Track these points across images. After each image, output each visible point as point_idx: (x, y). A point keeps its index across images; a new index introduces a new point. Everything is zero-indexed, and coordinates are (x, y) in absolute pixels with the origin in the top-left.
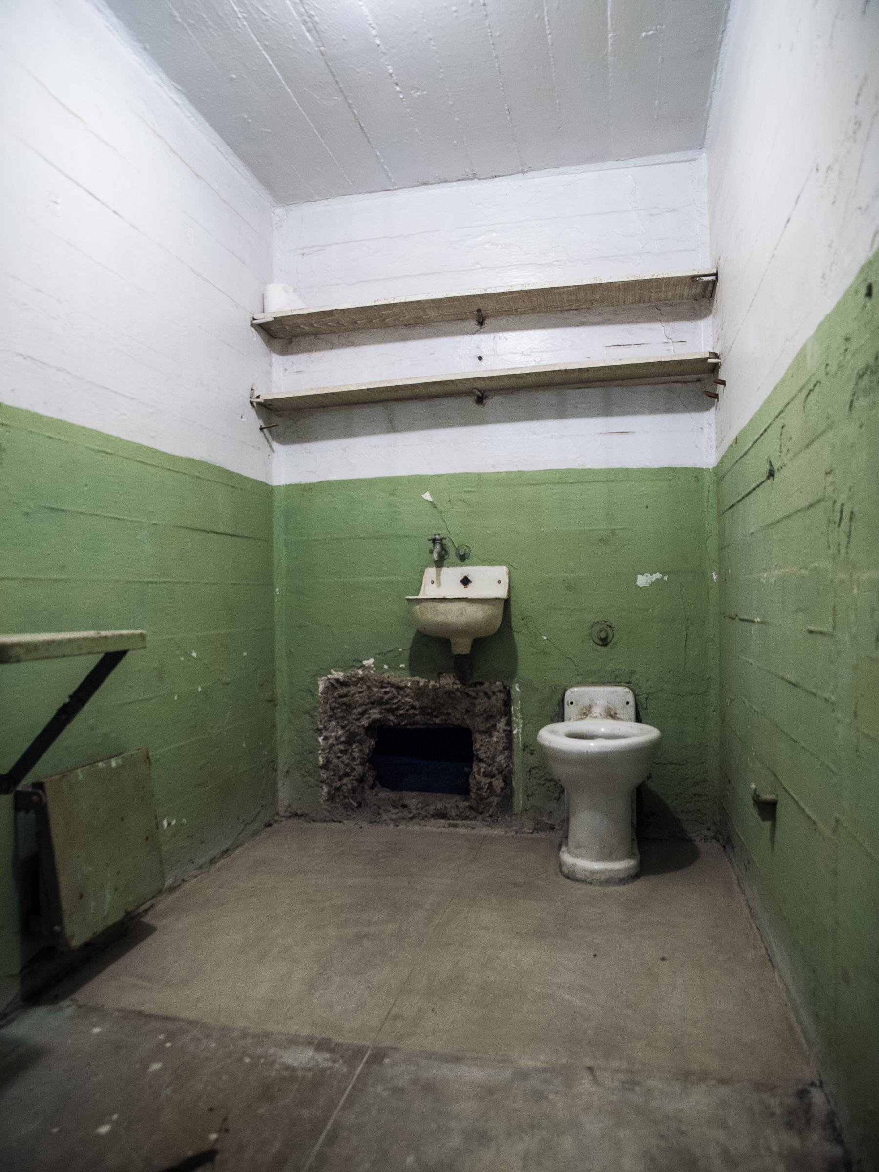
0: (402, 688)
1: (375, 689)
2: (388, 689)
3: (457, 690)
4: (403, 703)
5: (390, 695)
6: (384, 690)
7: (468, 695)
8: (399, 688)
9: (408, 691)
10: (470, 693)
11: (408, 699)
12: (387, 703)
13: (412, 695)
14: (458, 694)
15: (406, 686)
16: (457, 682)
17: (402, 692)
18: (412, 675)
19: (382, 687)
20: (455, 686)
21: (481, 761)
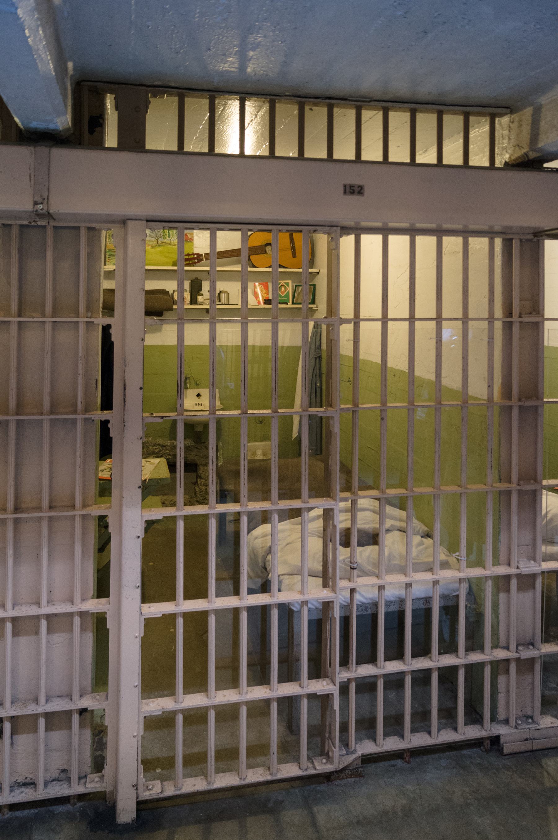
0: (165, 446)
1: (151, 447)
2: (157, 447)
3: (192, 446)
4: (165, 453)
5: (158, 450)
6: (155, 447)
7: (197, 448)
8: (163, 446)
9: (167, 447)
10: (198, 447)
11: (167, 451)
12: (157, 453)
13: (170, 449)
14: (192, 448)
15: (167, 446)
16: (193, 442)
17: (165, 448)
18: (171, 440)
19: (154, 446)
20: (192, 444)
21: (203, 479)
